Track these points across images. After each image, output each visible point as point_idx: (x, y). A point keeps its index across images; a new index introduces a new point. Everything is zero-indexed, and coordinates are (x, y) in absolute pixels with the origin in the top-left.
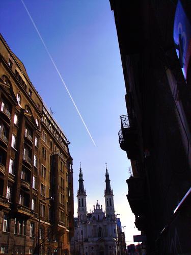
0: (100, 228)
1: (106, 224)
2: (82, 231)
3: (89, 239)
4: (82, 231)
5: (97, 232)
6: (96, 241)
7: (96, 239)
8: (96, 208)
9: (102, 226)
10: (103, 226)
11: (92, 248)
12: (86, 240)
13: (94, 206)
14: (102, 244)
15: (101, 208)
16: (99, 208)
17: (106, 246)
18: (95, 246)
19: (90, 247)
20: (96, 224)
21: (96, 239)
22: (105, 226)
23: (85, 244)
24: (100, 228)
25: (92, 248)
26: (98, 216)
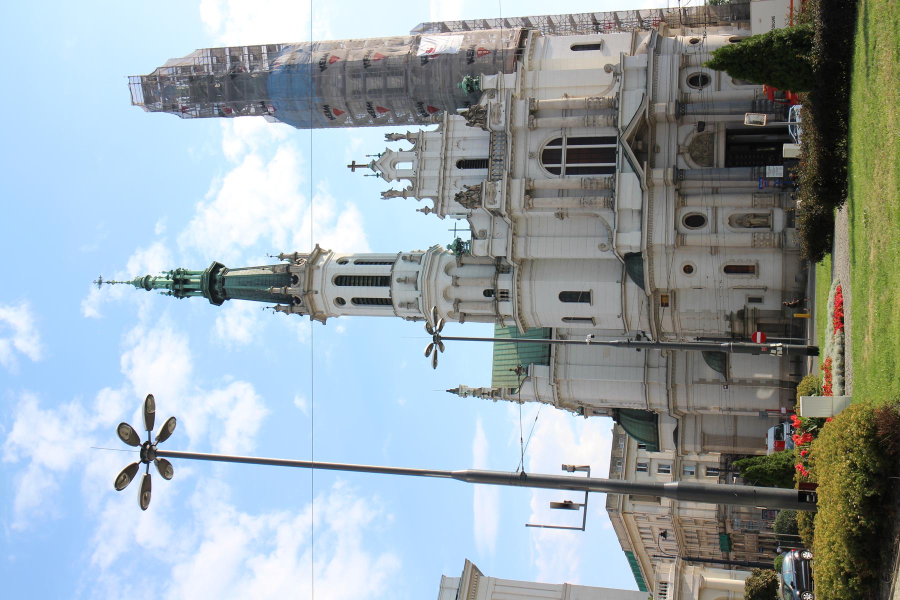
0: (549, 157)
1: (522, 109)
2: (565, 297)
3: (631, 241)
4: (565, 297)
5: (575, 179)
6: (647, 188)
7: (628, 185)
8: (405, 184)
9: (538, 142)
10: (532, 128)
11: (695, 221)
12: (633, 265)
13: (389, 194)
14: (670, 141)
15: (407, 145)
16: (401, 155)
17: (682, 107)
18: (682, 195)
19: (680, 242)
20: (518, 187)
21: (628, 185)
22: (534, 113)
23: (662, 273)
24: (549, 157)
25: (695, 221)
26: (463, 164)
